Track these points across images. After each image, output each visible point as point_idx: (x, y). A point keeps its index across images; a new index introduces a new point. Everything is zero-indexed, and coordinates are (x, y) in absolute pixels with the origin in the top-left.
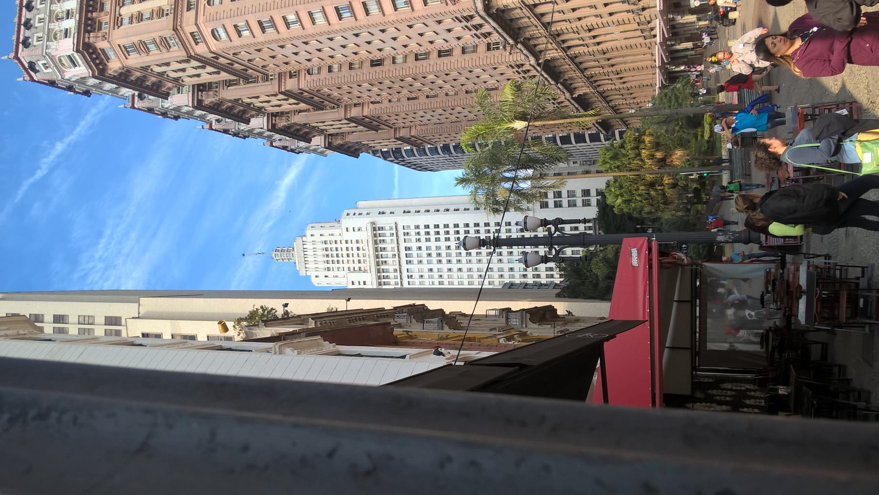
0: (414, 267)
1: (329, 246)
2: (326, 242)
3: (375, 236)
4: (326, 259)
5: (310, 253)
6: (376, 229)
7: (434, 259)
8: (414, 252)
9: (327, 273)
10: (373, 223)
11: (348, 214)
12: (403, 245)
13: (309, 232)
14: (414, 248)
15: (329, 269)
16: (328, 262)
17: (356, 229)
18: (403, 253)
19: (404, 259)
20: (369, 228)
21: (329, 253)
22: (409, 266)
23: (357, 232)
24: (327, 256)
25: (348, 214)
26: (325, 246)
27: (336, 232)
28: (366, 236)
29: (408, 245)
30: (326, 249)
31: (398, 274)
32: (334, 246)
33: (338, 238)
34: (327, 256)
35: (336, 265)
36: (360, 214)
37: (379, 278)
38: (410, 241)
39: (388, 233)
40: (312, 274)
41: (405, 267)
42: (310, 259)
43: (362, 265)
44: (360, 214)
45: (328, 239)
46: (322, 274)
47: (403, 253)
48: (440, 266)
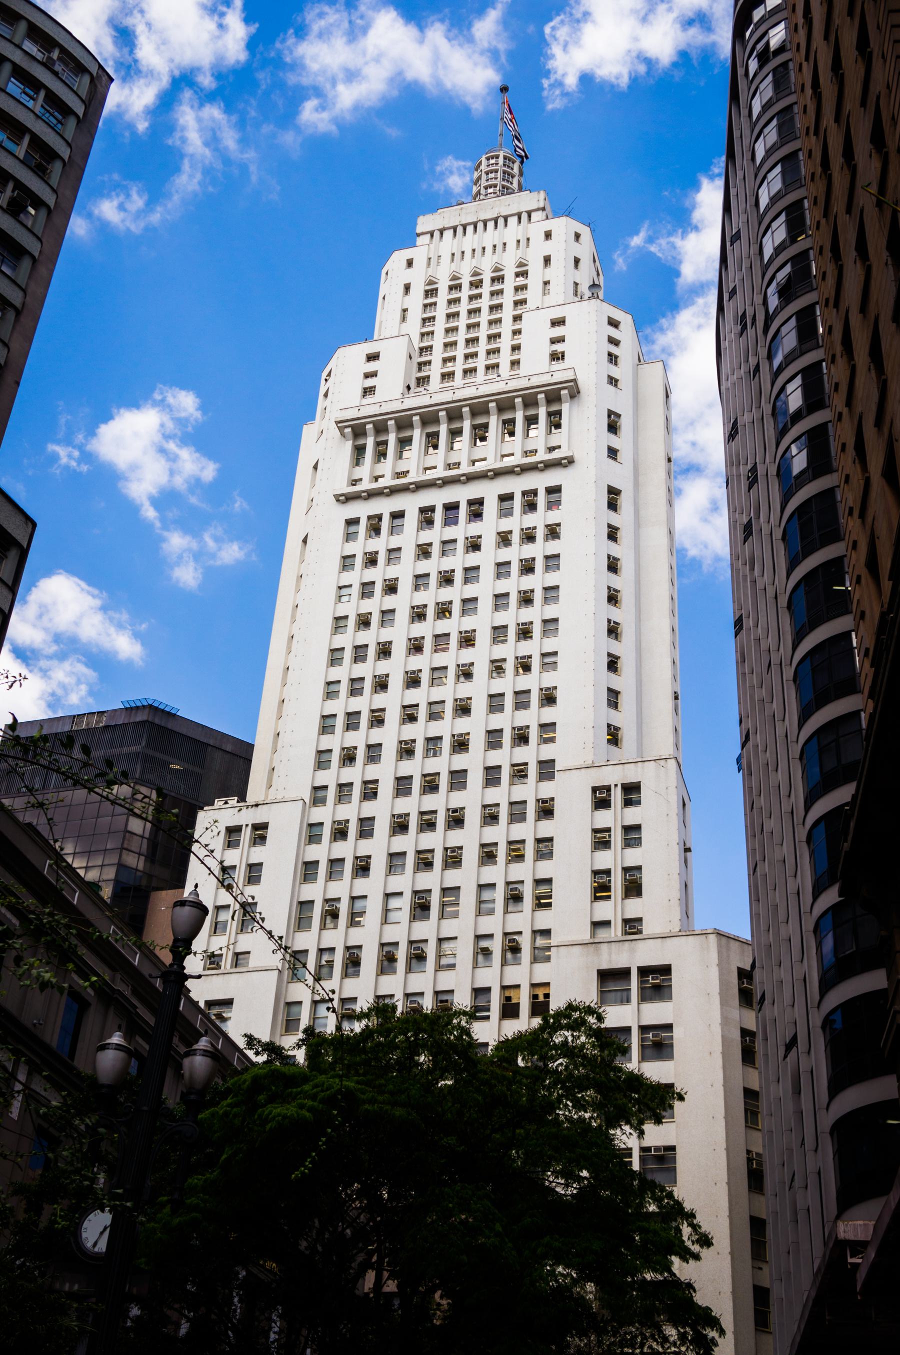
0: (409, 536)
1: (510, 283)
3: (530, 402)
4: (465, 281)
5: (490, 237)
7: (430, 597)
8: (462, 530)
10: (575, 393)
11: (614, 323)
12: (489, 491)
13: (563, 226)
14: (475, 529)
15: (431, 292)
17: (559, 347)
18: (462, 494)
19: (438, 498)
20: (559, 377)
22: (412, 519)
23: (548, 349)
25: (614, 323)
26: (509, 273)
28: (536, 370)
29: (491, 508)
30: (498, 279)
32: (508, 299)
35: (441, 312)
36: (613, 359)
37: (381, 428)
38: (505, 512)
40: (420, 252)
41: (411, 504)
42: (470, 241)
45: (534, 282)
46: (418, 279)
47: (462, 494)
48: (403, 615)
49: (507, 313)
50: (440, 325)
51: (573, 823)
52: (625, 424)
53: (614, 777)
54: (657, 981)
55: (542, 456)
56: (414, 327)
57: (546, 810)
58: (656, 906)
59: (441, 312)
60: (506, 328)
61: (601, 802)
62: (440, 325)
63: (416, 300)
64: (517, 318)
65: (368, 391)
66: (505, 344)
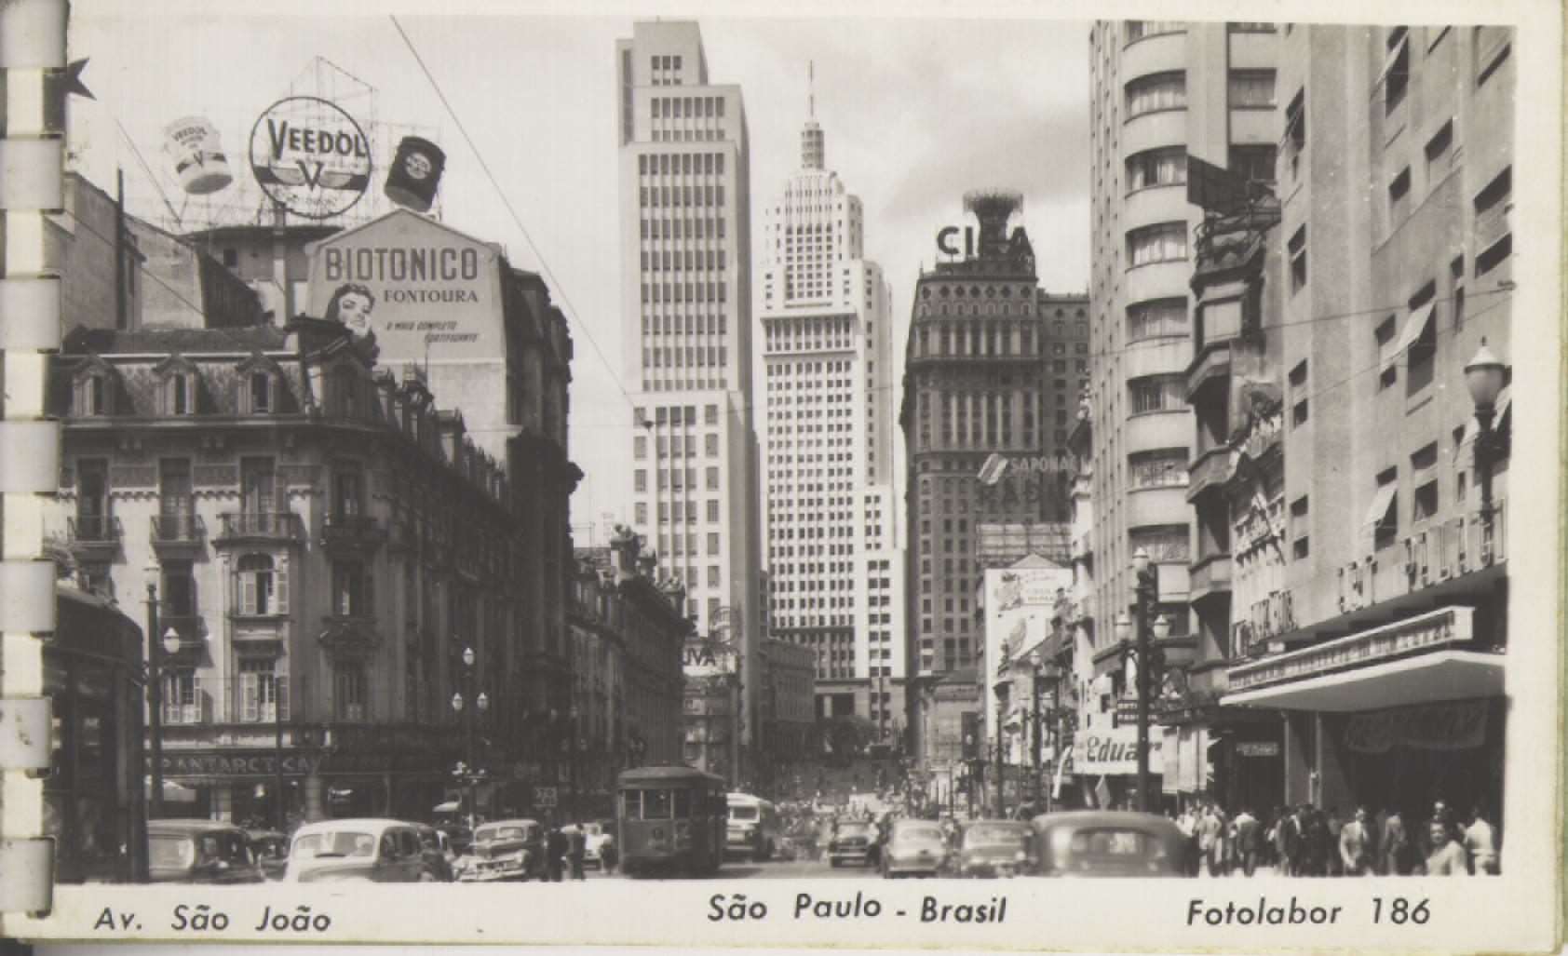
1: (824, 234)
2: (829, 229)
6: (845, 322)
9: (783, 231)
10: (855, 316)
15: (789, 231)
16: (800, 231)
20: (849, 310)
21: (814, 235)
24: (809, 230)
27: (844, 248)
28: (838, 308)
30: (819, 230)
31: (783, 351)
33: (835, 253)
34: (809, 230)
35: (795, 245)
38: (830, 369)
39: (842, 337)
43: (796, 290)
44: (869, 292)
49: (824, 253)
50: (795, 254)
51: (858, 508)
52: (875, 328)
53: (872, 492)
54: (885, 565)
55: (843, 348)
56: (782, 252)
57: (850, 501)
58: (885, 538)
59: (795, 245)
60: (824, 261)
61: (868, 500)
62: (795, 254)
63: (782, 235)
64: (829, 257)
65: (769, 296)
66: (824, 271)
